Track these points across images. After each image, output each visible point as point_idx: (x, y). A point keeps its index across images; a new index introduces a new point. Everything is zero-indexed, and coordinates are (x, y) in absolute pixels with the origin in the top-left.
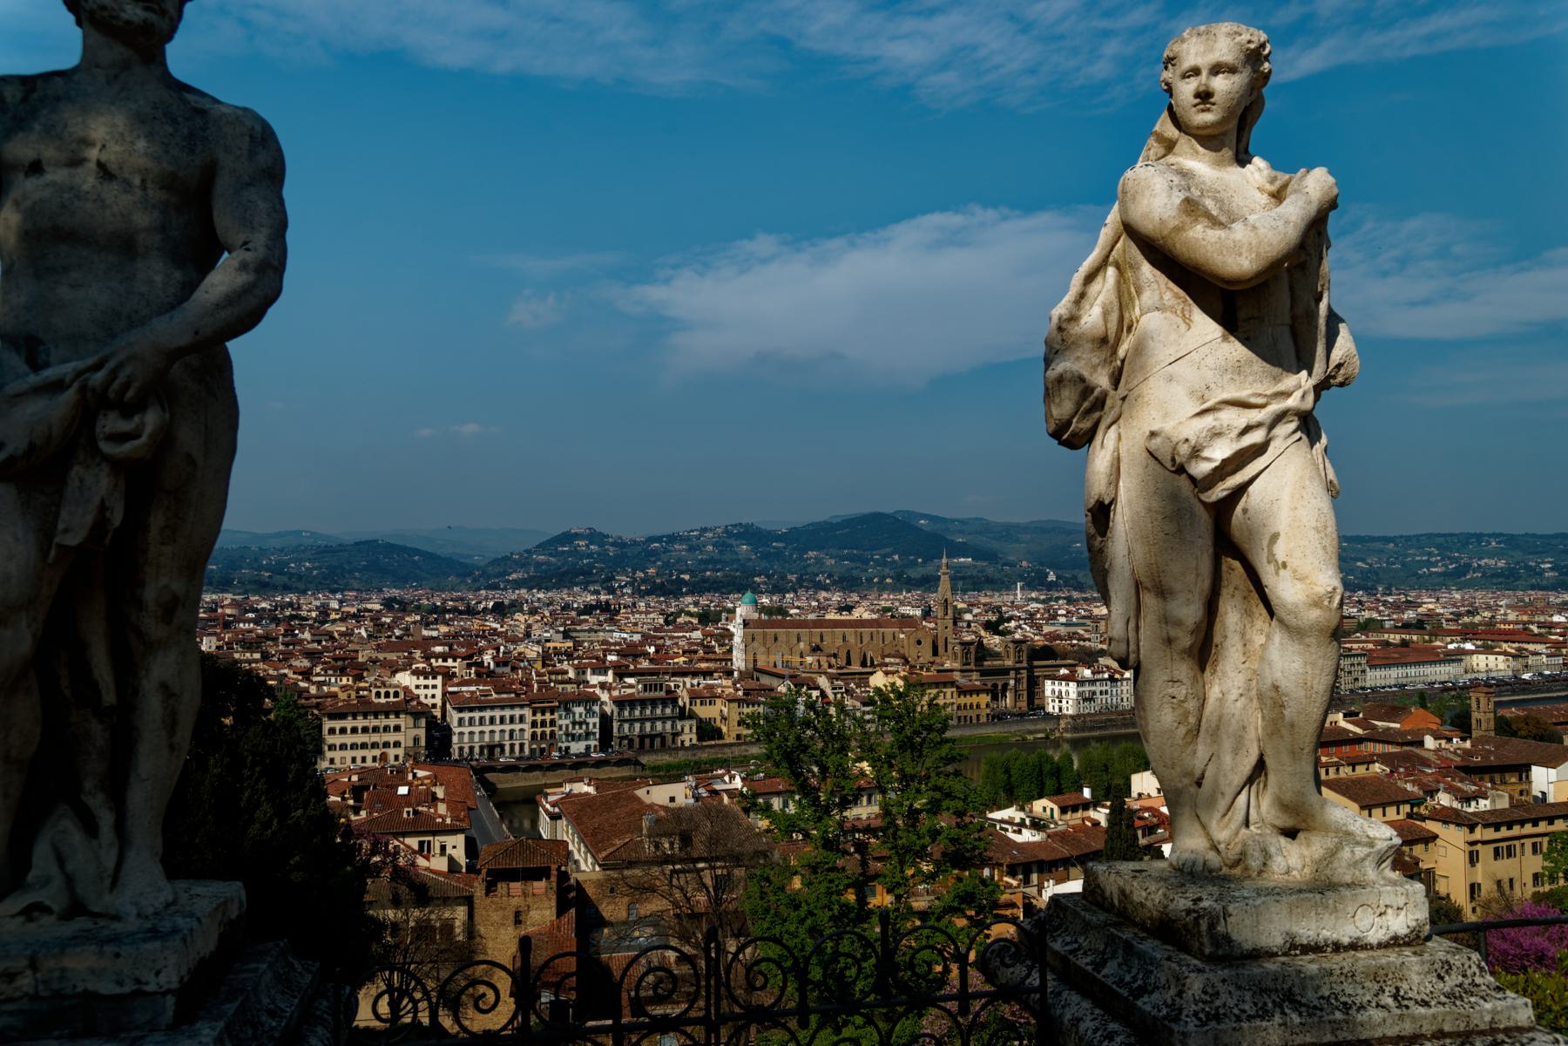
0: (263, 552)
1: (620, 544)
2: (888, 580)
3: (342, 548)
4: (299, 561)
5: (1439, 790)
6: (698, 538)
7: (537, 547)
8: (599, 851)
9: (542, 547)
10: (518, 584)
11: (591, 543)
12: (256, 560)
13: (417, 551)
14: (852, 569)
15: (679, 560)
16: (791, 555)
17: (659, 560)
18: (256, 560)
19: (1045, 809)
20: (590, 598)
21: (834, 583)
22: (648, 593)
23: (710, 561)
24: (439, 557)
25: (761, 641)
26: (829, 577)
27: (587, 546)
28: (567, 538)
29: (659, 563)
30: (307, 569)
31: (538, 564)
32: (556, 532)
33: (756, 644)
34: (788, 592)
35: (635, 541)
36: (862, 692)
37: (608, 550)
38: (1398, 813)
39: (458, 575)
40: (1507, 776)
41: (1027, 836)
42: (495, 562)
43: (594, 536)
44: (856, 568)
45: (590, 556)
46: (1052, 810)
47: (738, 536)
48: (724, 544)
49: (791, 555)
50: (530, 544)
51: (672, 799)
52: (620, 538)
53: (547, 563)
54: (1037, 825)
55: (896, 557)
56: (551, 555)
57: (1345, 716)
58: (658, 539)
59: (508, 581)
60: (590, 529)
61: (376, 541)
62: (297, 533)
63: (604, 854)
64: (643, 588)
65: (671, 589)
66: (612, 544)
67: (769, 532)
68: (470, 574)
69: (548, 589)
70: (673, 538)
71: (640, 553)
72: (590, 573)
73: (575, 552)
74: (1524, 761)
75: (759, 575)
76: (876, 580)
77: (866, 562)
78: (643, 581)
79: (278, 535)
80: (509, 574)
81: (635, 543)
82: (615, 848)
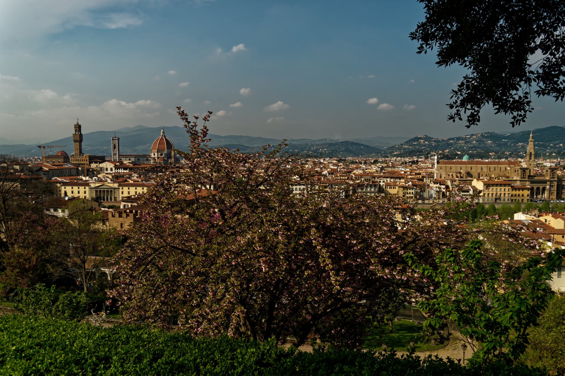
0: (312, 145)
1: (437, 141)
2: (553, 154)
3: (337, 144)
4: (323, 148)
6: (469, 138)
9: (407, 143)
10: (395, 156)
11: (425, 141)
12: (310, 148)
13: (363, 145)
14: (539, 150)
15: (461, 147)
16: (511, 144)
17: (452, 147)
18: (310, 148)
23: (475, 147)
24: (371, 147)
25: (444, 169)
27: (424, 142)
28: (417, 139)
29: (453, 148)
30: (325, 151)
31: (405, 149)
32: (412, 137)
33: (441, 171)
39: (376, 153)
42: (389, 148)
43: (427, 138)
44: (541, 150)
45: (425, 146)
47: (487, 137)
48: (480, 141)
49: (511, 144)
50: (403, 141)
52: (437, 139)
53: (408, 148)
56: (410, 145)
58: (453, 139)
59: (392, 155)
60: (425, 136)
61: (348, 141)
62: (326, 139)
66: (434, 141)
67: (501, 136)
68: (380, 153)
70: (459, 139)
71: (445, 144)
72: (422, 152)
73: (419, 144)
75: (492, 152)
76: (547, 154)
77: (547, 147)
79: (320, 140)
81: (443, 141)
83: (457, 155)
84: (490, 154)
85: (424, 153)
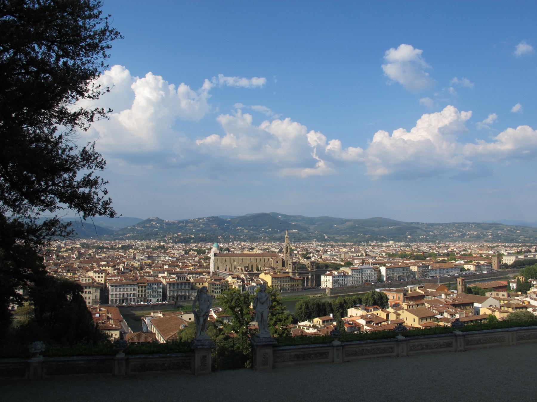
5: (444, 312)
6: (197, 222)
7: (138, 224)
8: (165, 337)
10: (129, 238)
15: (190, 229)
19: (317, 321)
20: (157, 244)
21: (248, 239)
22: (178, 242)
26: (245, 237)
27: (156, 224)
31: (138, 230)
33: (218, 262)
34: (230, 242)
35: (174, 223)
36: (257, 280)
37: (164, 226)
38: (431, 320)
40: (466, 307)
41: (312, 331)
42: (122, 230)
43: (158, 220)
45: (157, 228)
46: (320, 322)
51: (190, 319)
54: (315, 327)
55: (270, 229)
56: (142, 227)
57: (419, 288)
58: (182, 222)
59: (127, 237)
63: (167, 338)
64: (177, 240)
65: (187, 241)
67: (224, 220)
69: (141, 240)
70: (187, 222)
74: (471, 302)
76: (262, 238)
78: (177, 238)
80: (127, 235)
81: (174, 223)
82: (171, 336)
83: (191, 238)
84: (219, 237)
85: (160, 236)
